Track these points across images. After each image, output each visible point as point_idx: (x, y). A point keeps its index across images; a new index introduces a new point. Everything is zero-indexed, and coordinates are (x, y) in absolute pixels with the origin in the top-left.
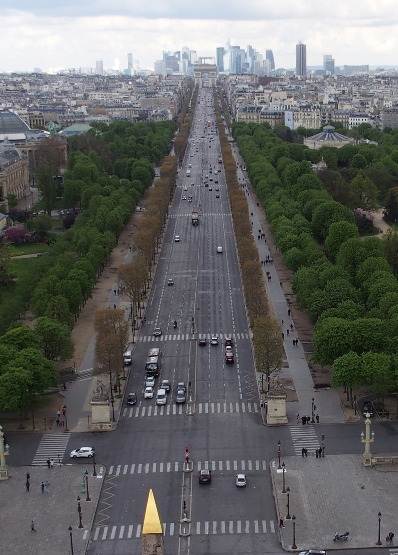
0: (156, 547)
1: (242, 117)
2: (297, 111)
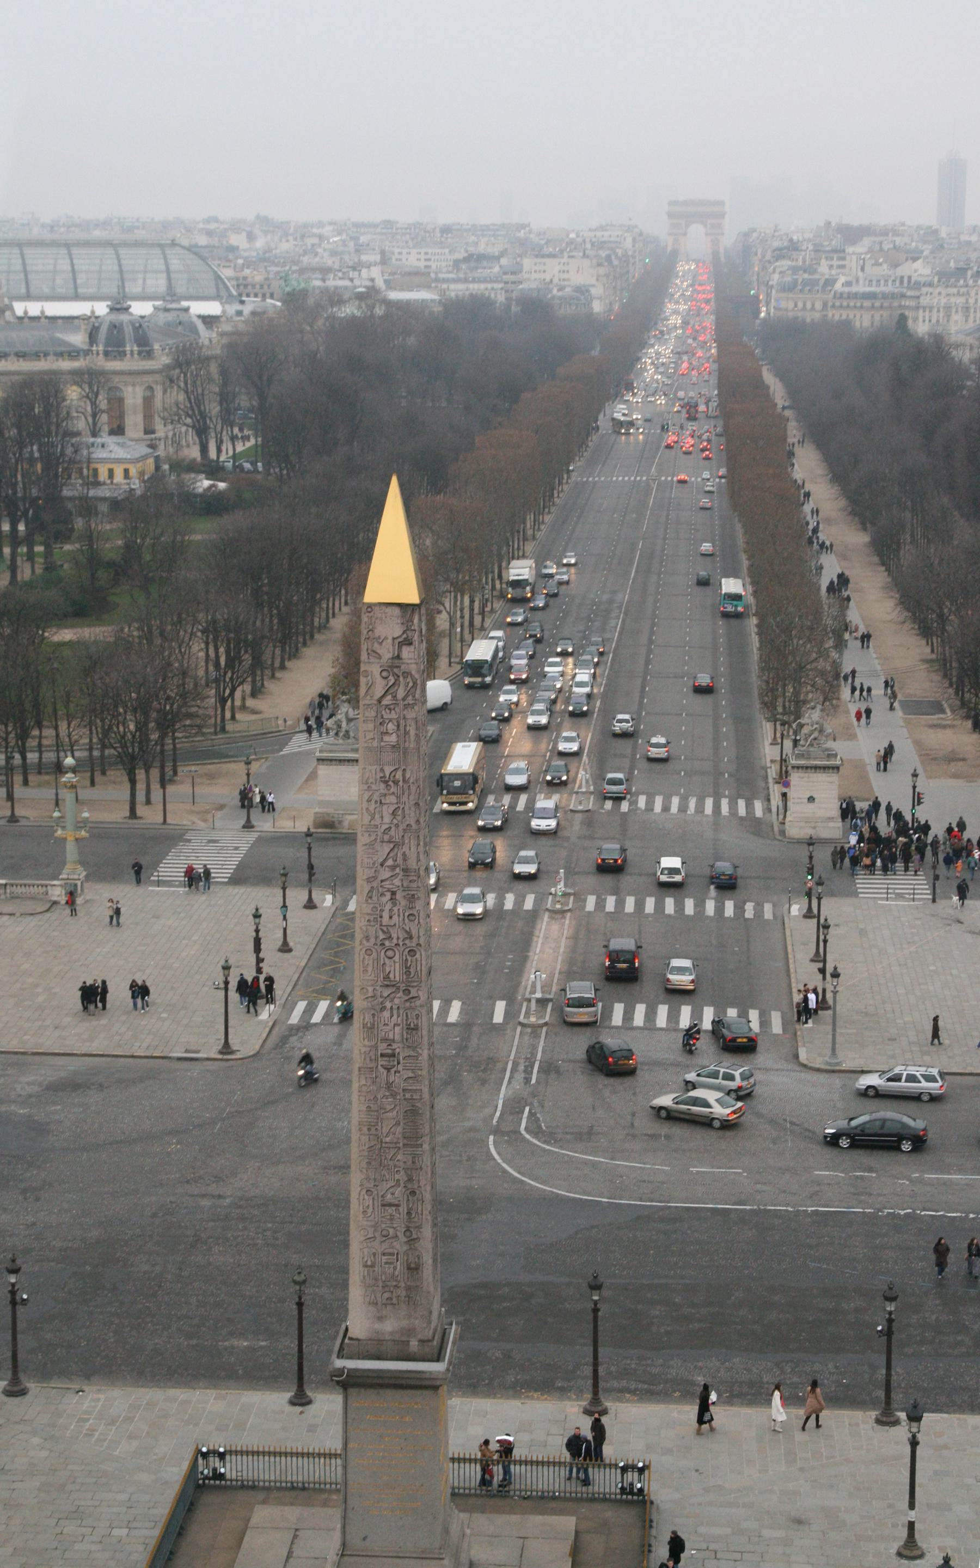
0: (401, 644)
1: (783, 304)
2: (930, 285)
